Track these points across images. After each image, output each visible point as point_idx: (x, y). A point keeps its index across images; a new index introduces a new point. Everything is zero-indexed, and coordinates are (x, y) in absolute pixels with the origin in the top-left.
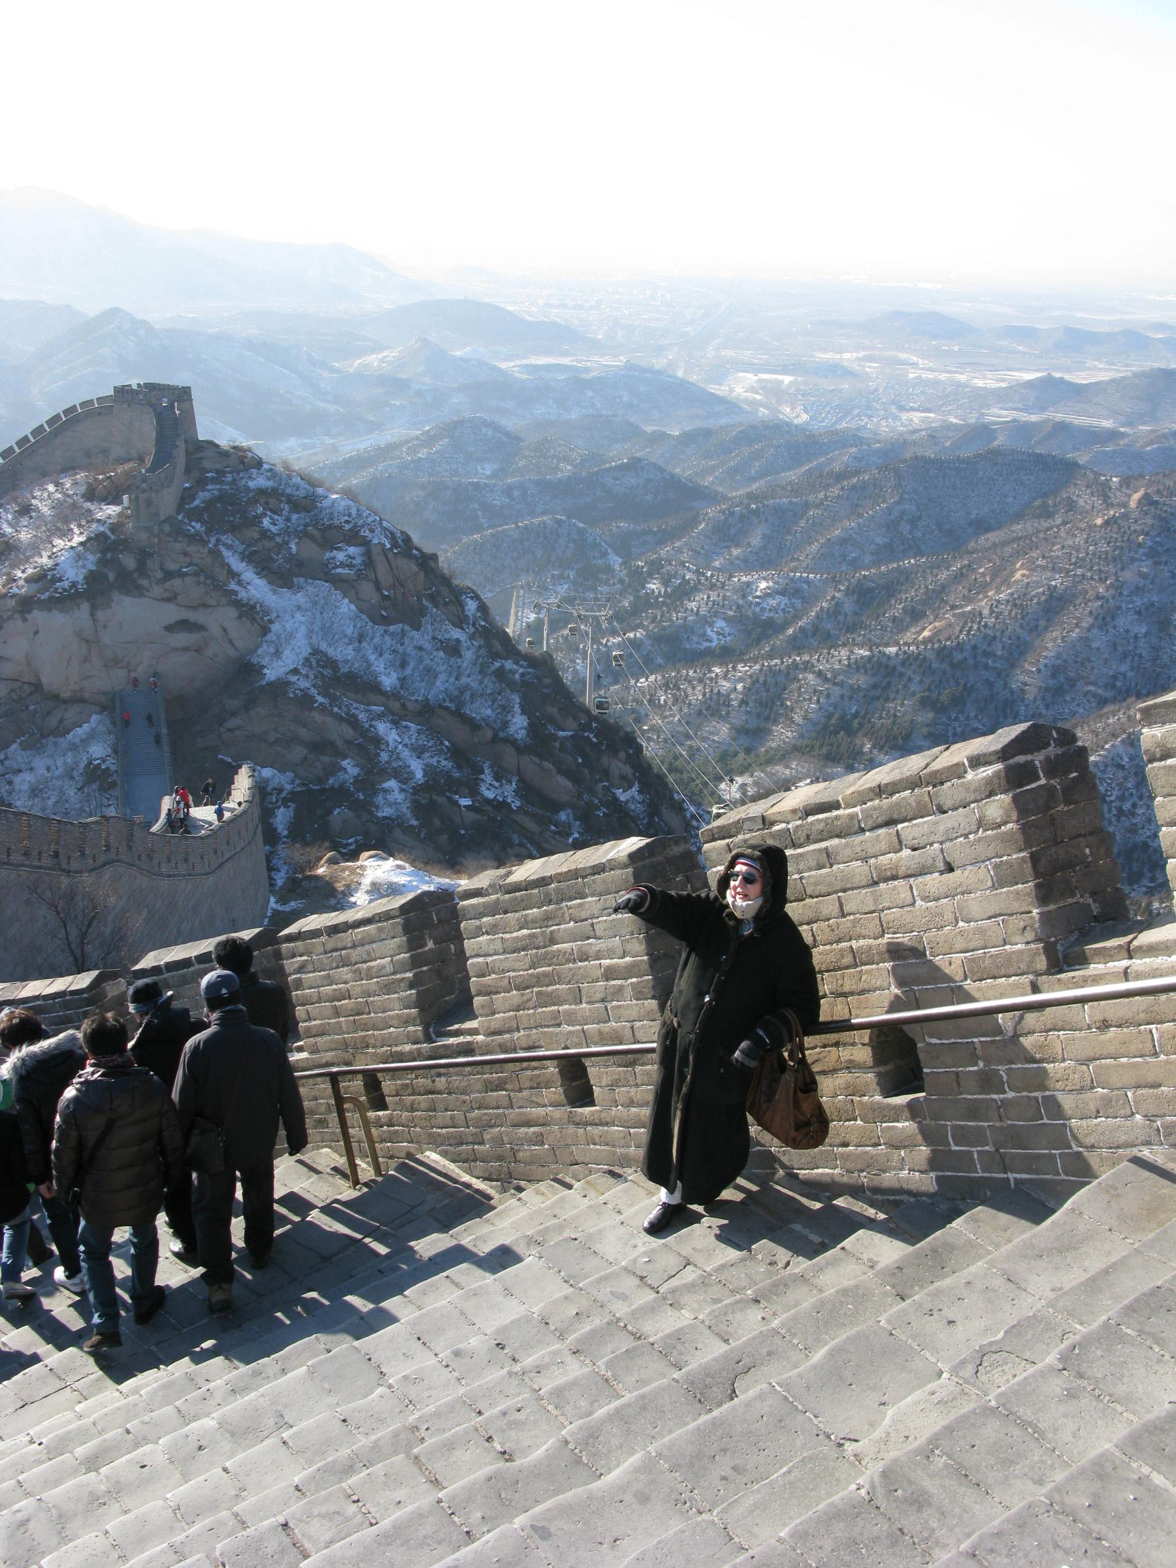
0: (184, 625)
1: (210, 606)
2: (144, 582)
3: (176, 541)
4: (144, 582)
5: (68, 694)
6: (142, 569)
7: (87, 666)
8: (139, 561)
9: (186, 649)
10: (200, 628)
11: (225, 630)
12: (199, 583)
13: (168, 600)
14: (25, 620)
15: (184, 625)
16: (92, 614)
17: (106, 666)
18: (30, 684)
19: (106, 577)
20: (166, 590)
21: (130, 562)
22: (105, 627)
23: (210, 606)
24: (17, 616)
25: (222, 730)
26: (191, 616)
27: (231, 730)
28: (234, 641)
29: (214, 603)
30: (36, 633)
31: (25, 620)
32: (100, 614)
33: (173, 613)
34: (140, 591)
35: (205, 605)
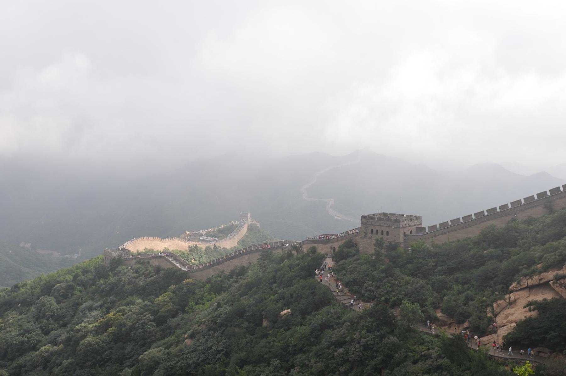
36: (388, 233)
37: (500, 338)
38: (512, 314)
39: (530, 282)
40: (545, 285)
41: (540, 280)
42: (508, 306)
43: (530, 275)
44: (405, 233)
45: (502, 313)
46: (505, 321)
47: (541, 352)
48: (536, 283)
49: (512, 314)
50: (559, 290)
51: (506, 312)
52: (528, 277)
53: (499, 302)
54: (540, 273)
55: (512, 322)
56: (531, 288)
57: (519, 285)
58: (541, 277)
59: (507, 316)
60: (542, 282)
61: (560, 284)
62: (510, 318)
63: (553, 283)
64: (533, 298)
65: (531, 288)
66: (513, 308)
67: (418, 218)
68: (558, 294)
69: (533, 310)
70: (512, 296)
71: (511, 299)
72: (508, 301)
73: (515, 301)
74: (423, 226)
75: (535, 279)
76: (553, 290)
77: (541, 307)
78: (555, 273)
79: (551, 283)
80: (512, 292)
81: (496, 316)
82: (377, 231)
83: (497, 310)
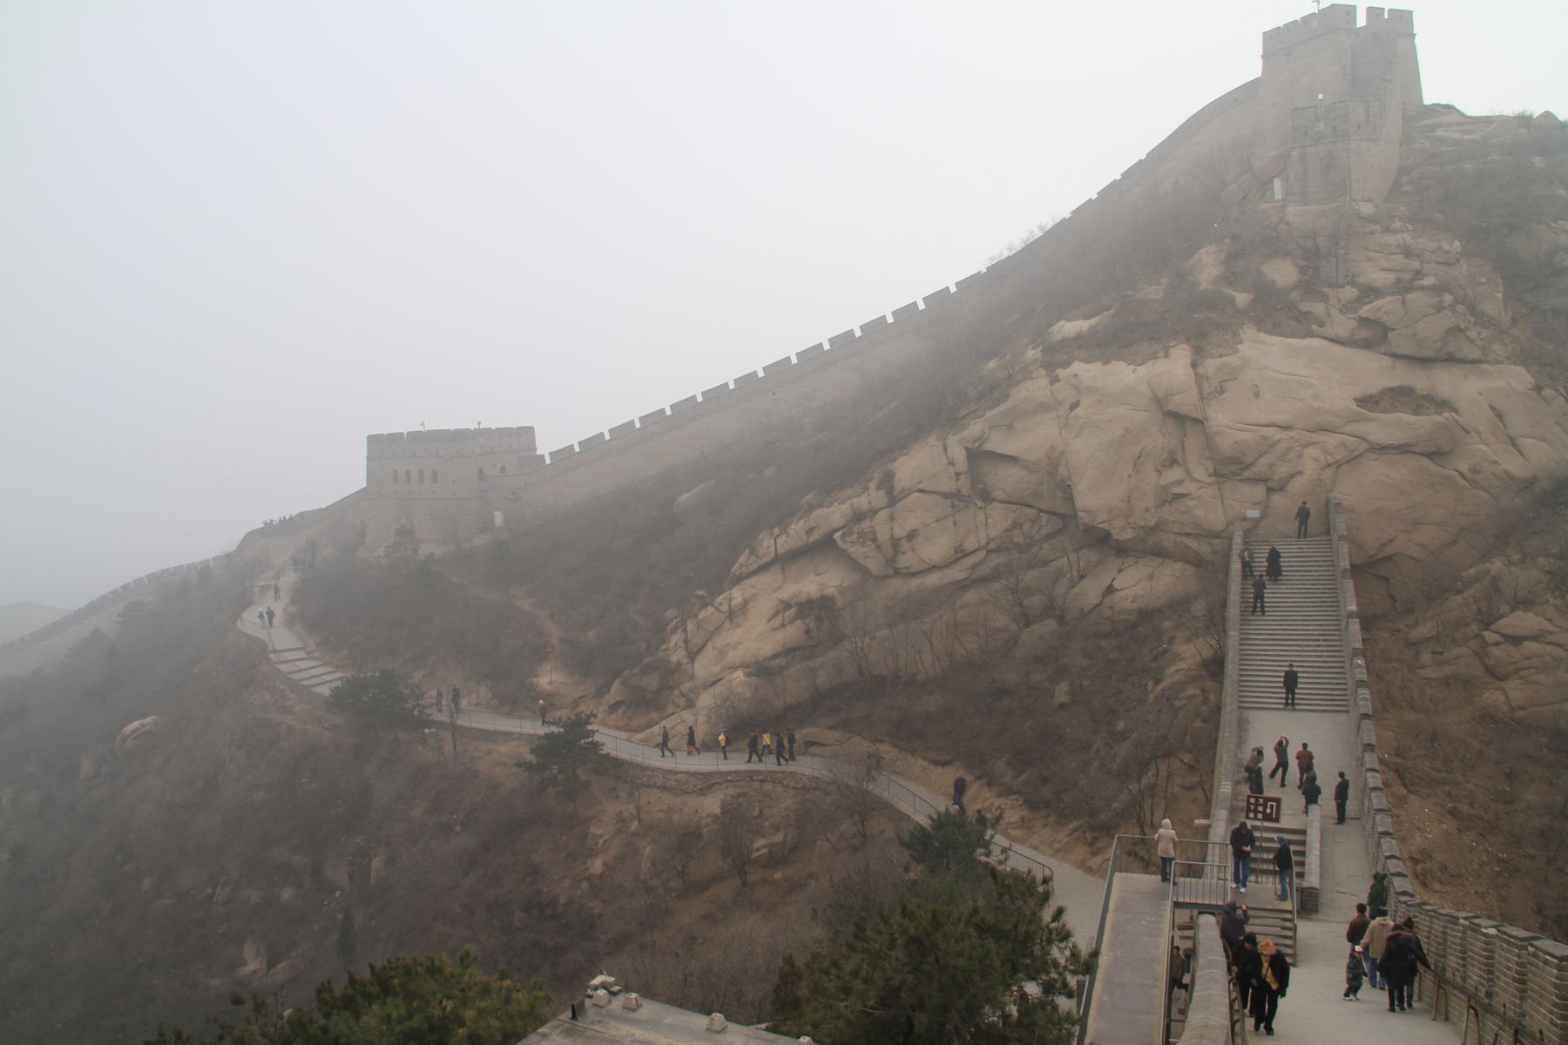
0: (1401, 397)
1: (1463, 361)
2: (1317, 308)
3: (1387, 230)
4: (1317, 308)
5: (1128, 535)
6: (1310, 286)
7: (1175, 474)
8: (1302, 270)
9: (1404, 449)
10: (1443, 404)
11: (1500, 416)
12: (1439, 309)
13: (1367, 345)
14: (1055, 380)
15: (1401, 397)
16: (1194, 365)
17: (1217, 474)
18: (1052, 513)
19: (1232, 301)
20: (1365, 321)
21: (1282, 273)
22: (1222, 391)
23: (1463, 361)
24: (1043, 372)
25: (1490, 636)
26: (1419, 380)
27: (1516, 640)
28: (1523, 442)
29: (1474, 353)
30: (1074, 406)
31: (1055, 380)
32: (1211, 365)
33: (1376, 372)
34: (1303, 325)
35: (1451, 359)
36: (435, 475)
37: (702, 719)
38: (735, 646)
39: (785, 544)
40: (823, 547)
41: (809, 531)
42: (727, 625)
43: (783, 522)
44: (481, 470)
45: (710, 646)
46: (717, 669)
47: (814, 743)
48: (799, 544)
49: (735, 646)
50: (856, 551)
51: (719, 642)
52: (776, 531)
53: (702, 614)
54: (811, 509)
55: (734, 668)
56: (785, 560)
57: (753, 558)
58: (812, 523)
59: (722, 653)
60: (812, 539)
61: (862, 535)
62: (734, 656)
63: (843, 536)
64: (787, 592)
65: (785, 560)
66: (738, 626)
67: (527, 433)
68: (855, 565)
69: (791, 622)
70: (737, 595)
71: (734, 603)
72: (725, 608)
73: (746, 603)
74: (539, 452)
75: (795, 534)
76: (844, 556)
77: (818, 609)
78: (846, 506)
79: (837, 536)
80: (739, 580)
81: (693, 656)
82: (408, 473)
83: (697, 641)
